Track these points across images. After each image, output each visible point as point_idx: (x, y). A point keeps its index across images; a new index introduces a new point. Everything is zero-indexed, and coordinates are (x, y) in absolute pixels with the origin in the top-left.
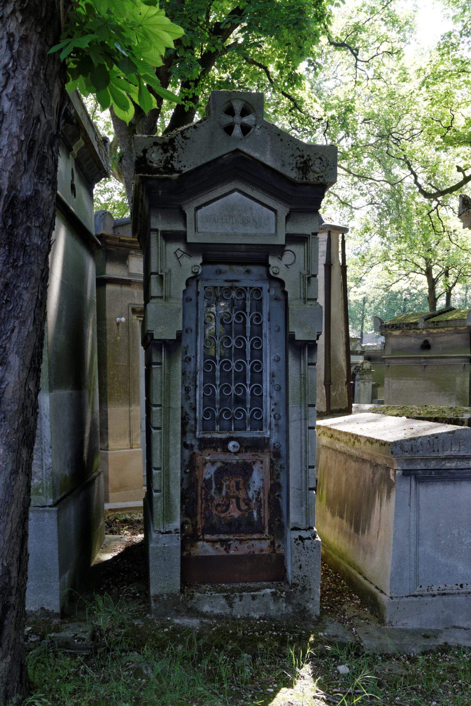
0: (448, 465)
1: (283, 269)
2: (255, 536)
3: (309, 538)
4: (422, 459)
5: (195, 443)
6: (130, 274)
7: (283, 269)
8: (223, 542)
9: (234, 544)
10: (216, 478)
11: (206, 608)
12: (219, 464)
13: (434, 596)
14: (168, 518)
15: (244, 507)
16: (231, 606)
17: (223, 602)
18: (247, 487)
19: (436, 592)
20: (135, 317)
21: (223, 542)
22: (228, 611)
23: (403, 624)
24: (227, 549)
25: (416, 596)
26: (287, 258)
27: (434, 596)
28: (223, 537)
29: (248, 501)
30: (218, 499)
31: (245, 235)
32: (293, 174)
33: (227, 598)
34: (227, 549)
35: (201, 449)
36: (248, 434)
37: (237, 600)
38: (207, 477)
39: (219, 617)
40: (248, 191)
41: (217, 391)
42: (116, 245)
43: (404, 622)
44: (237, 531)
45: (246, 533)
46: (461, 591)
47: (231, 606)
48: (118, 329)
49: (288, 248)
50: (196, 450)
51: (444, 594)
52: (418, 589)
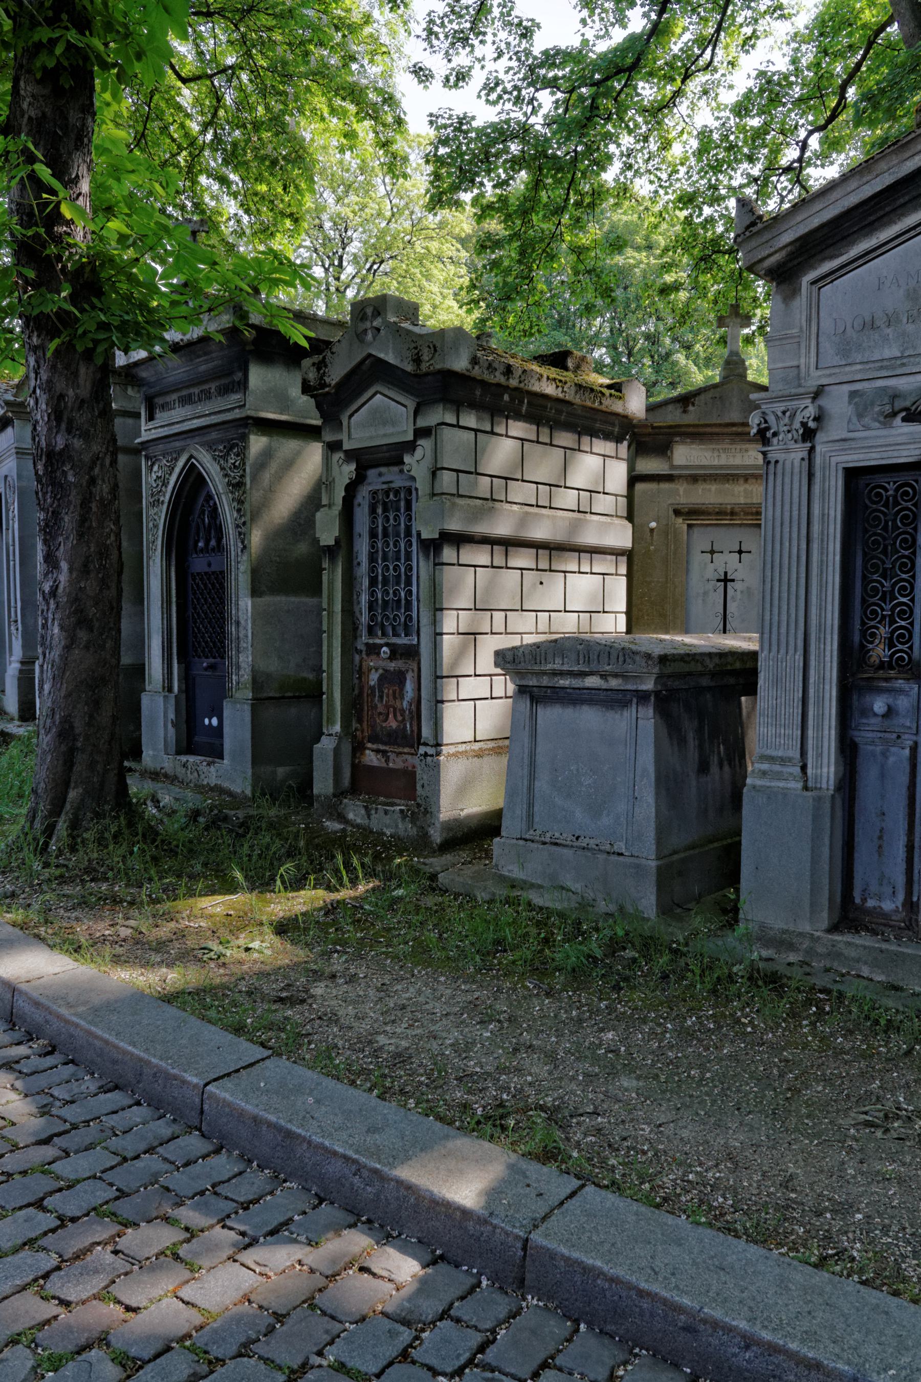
0: (561, 682)
1: (415, 465)
2: (406, 750)
3: (432, 756)
4: (532, 674)
5: (363, 648)
6: (673, 467)
7: (415, 465)
8: (384, 753)
9: (392, 756)
10: (379, 685)
11: (351, 816)
12: (381, 671)
13: (544, 843)
14: (331, 721)
15: (400, 718)
16: (369, 817)
17: (363, 812)
18: (402, 698)
19: (548, 840)
20: (680, 520)
21: (384, 753)
22: (367, 821)
23: (509, 871)
24: (387, 761)
25: (526, 840)
26: (419, 452)
27: (544, 843)
28: (382, 747)
29: (402, 711)
30: (380, 708)
31: (385, 435)
32: (409, 368)
33: (366, 808)
34: (387, 761)
35: (368, 655)
36: (402, 640)
37: (373, 812)
38: (372, 683)
39: (358, 826)
40: (386, 392)
41: (380, 596)
42: (650, 434)
43: (510, 868)
44: (395, 743)
45: (399, 745)
46: (575, 844)
47: (369, 817)
48: (652, 536)
49: (419, 443)
50: (364, 656)
51: (556, 844)
52: (531, 832)
